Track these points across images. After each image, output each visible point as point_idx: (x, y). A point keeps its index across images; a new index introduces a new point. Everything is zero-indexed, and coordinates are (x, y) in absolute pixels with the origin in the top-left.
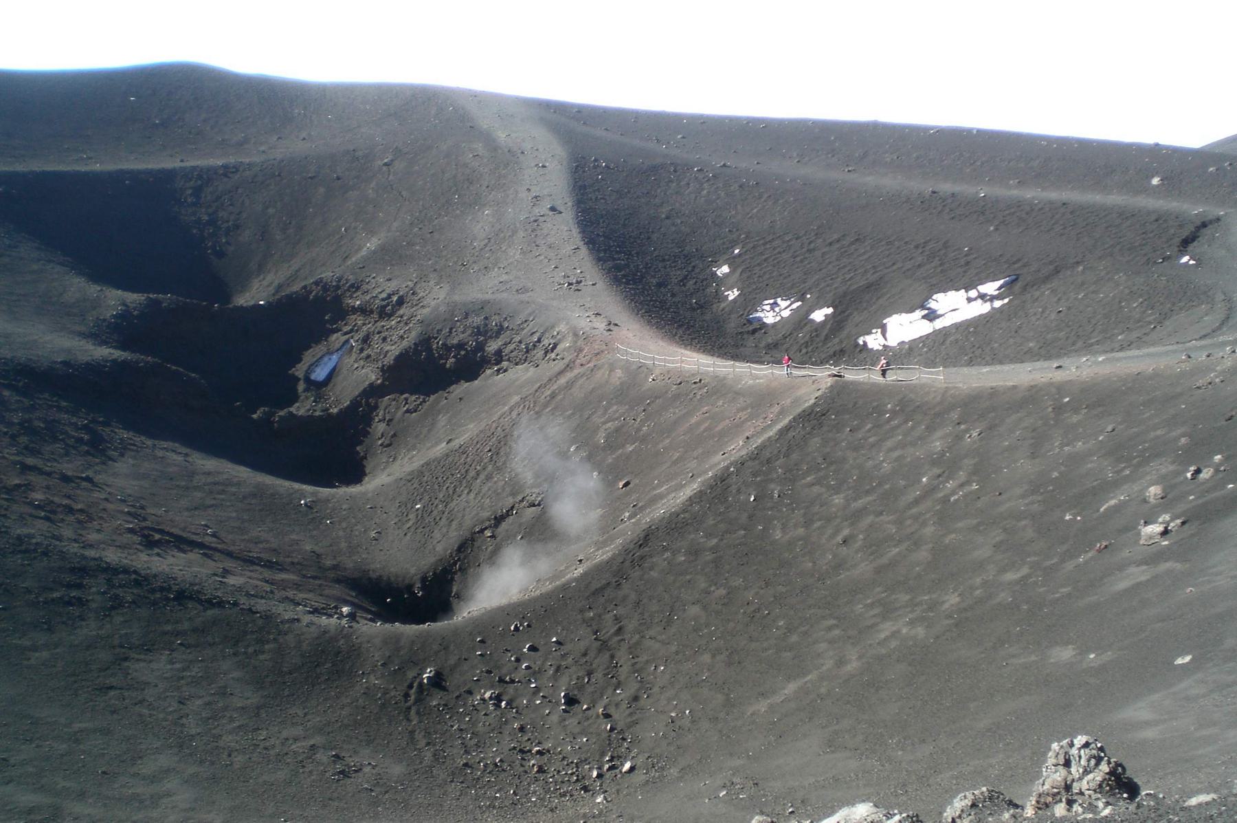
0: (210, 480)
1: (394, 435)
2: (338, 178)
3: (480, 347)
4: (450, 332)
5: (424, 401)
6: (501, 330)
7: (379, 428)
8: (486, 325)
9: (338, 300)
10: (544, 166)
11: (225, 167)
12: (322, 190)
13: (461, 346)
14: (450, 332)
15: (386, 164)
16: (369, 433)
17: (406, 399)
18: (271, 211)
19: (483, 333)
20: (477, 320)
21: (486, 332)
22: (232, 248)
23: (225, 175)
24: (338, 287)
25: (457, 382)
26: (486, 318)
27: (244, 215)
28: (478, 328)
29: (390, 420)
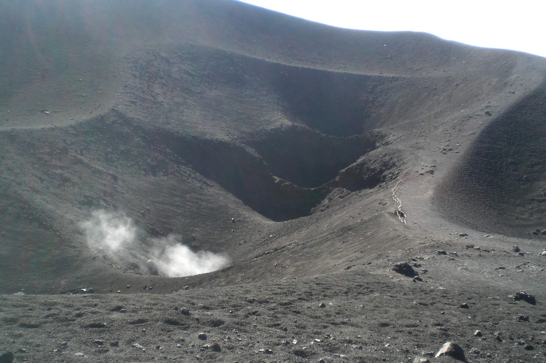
0: (199, 197)
1: (328, 207)
2: (435, 89)
3: (382, 171)
4: (374, 162)
5: (349, 194)
6: (394, 165)
7: (326, 201)
8: (389, 161)
9: (374, 142)
10: (514, 93)
11: (393, 78)
12: (426, 94)
13: (374, 170)
14: (374, 162)
15: (457, 85)
16: (320, 203)
17: (343, 191)
18: (400, 100)
19: (386, 166)
20: (387, 158)
21: (387, 165)
22: (374, 115)
23: (391, 82)
24: (377, 136)
25: (366, 188)
26: (391, 158)
27: (389, 101)
28: (385, 162)
29: (332, 199)
